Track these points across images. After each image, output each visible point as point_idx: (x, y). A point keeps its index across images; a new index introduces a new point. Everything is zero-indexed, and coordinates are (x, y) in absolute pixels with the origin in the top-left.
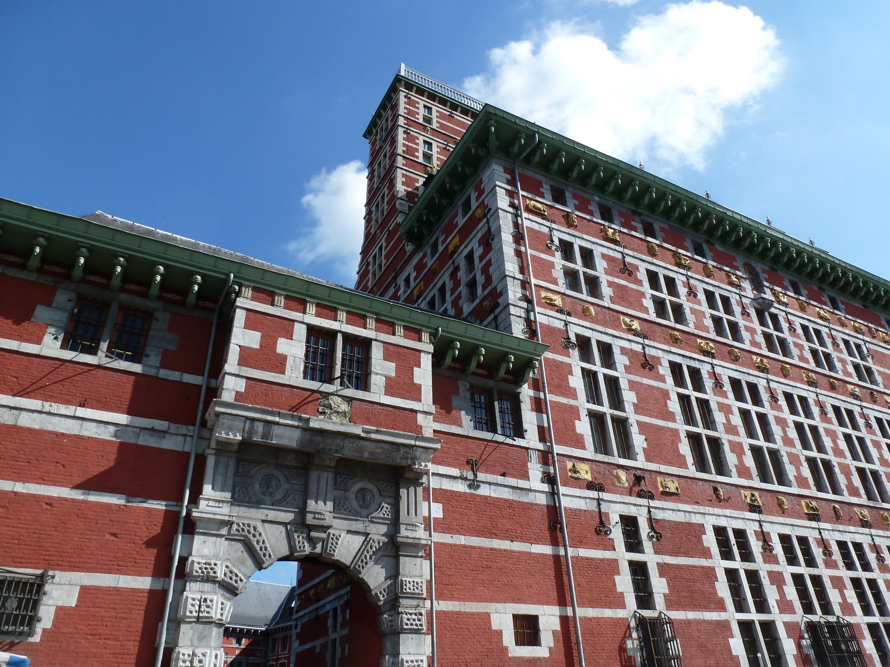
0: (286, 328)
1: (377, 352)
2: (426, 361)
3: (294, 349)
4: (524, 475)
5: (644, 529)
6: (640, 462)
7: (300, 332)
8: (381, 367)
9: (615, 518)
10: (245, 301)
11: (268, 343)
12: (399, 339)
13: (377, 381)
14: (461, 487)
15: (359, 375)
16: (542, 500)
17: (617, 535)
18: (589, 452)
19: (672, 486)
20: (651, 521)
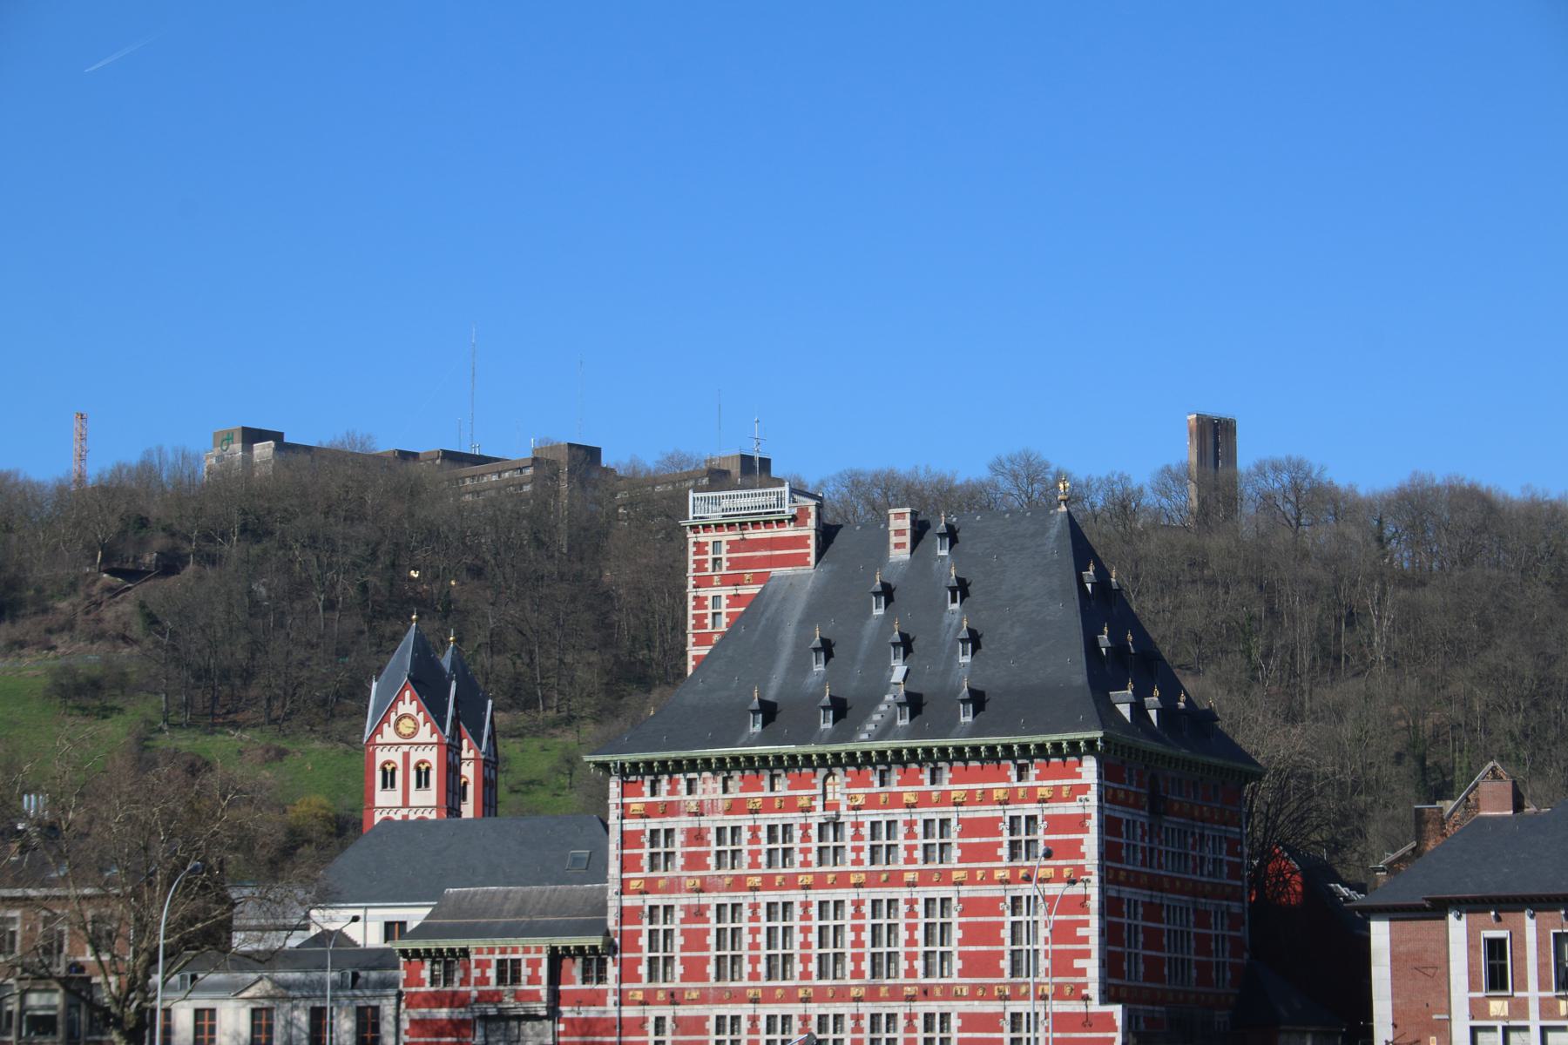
0: (487, 964)
1: (524, 964)
2: (545, 963)
3: (492, 973)
4: (604, 1004)
5: (669, 1023)
6: (677, 984)
7: (494, 963)
8: (525, 971)
9: (652, 1020)
10: (473, 957)
11: (483, 973)
12: (533, 956)
13: (524, 979)
14: (574, 1015)
15: (516, 979)
16: (616, 1015)
17: (651, 1027)
18: (645, 984)
19: (695, 995)
20: (675, 1019)
